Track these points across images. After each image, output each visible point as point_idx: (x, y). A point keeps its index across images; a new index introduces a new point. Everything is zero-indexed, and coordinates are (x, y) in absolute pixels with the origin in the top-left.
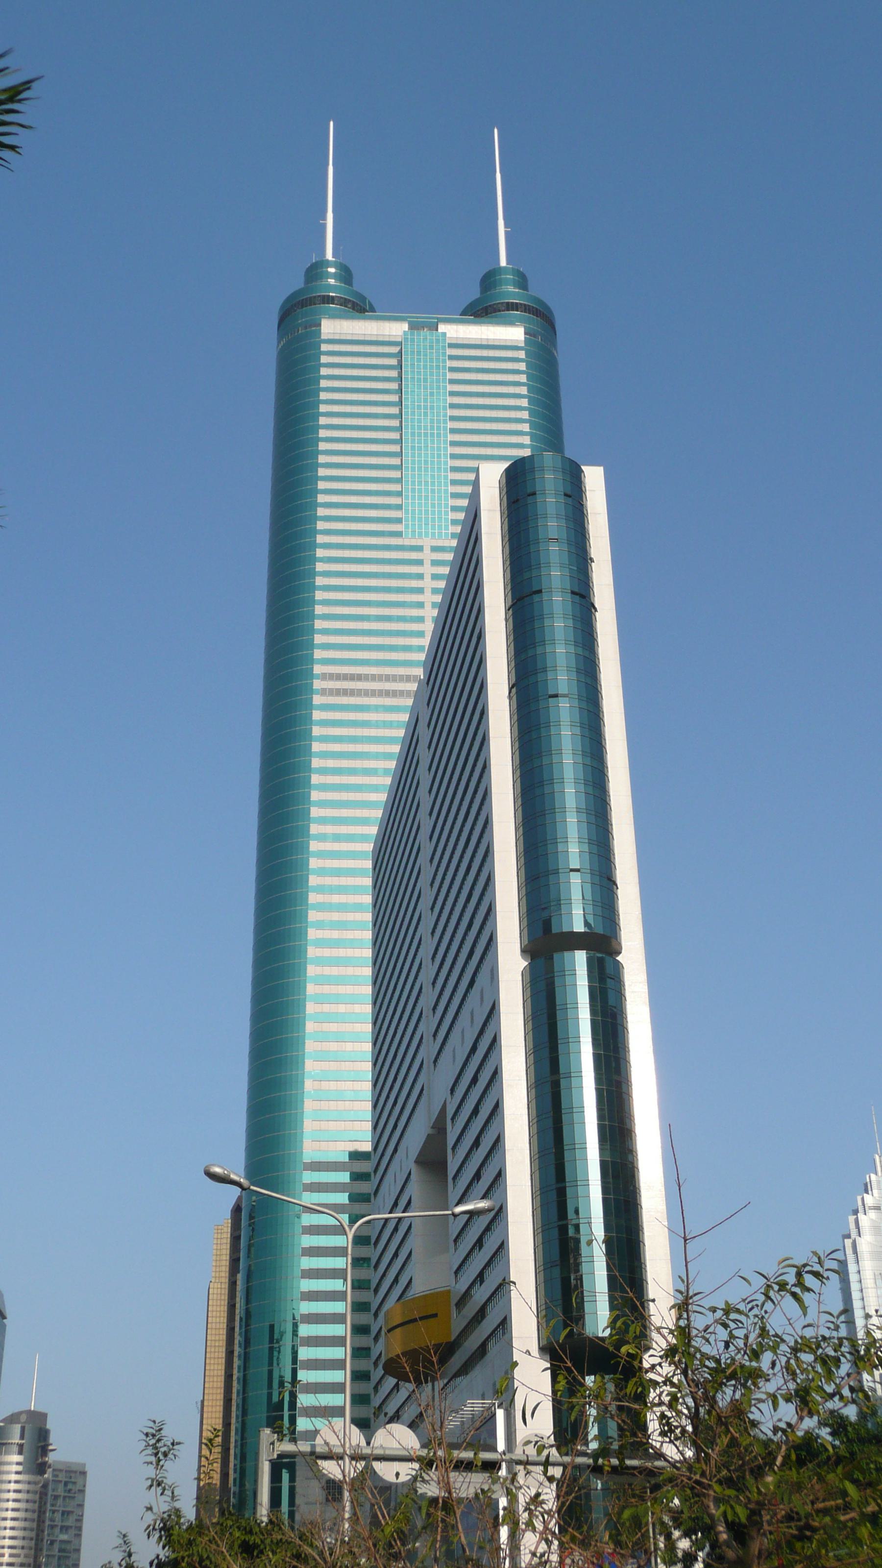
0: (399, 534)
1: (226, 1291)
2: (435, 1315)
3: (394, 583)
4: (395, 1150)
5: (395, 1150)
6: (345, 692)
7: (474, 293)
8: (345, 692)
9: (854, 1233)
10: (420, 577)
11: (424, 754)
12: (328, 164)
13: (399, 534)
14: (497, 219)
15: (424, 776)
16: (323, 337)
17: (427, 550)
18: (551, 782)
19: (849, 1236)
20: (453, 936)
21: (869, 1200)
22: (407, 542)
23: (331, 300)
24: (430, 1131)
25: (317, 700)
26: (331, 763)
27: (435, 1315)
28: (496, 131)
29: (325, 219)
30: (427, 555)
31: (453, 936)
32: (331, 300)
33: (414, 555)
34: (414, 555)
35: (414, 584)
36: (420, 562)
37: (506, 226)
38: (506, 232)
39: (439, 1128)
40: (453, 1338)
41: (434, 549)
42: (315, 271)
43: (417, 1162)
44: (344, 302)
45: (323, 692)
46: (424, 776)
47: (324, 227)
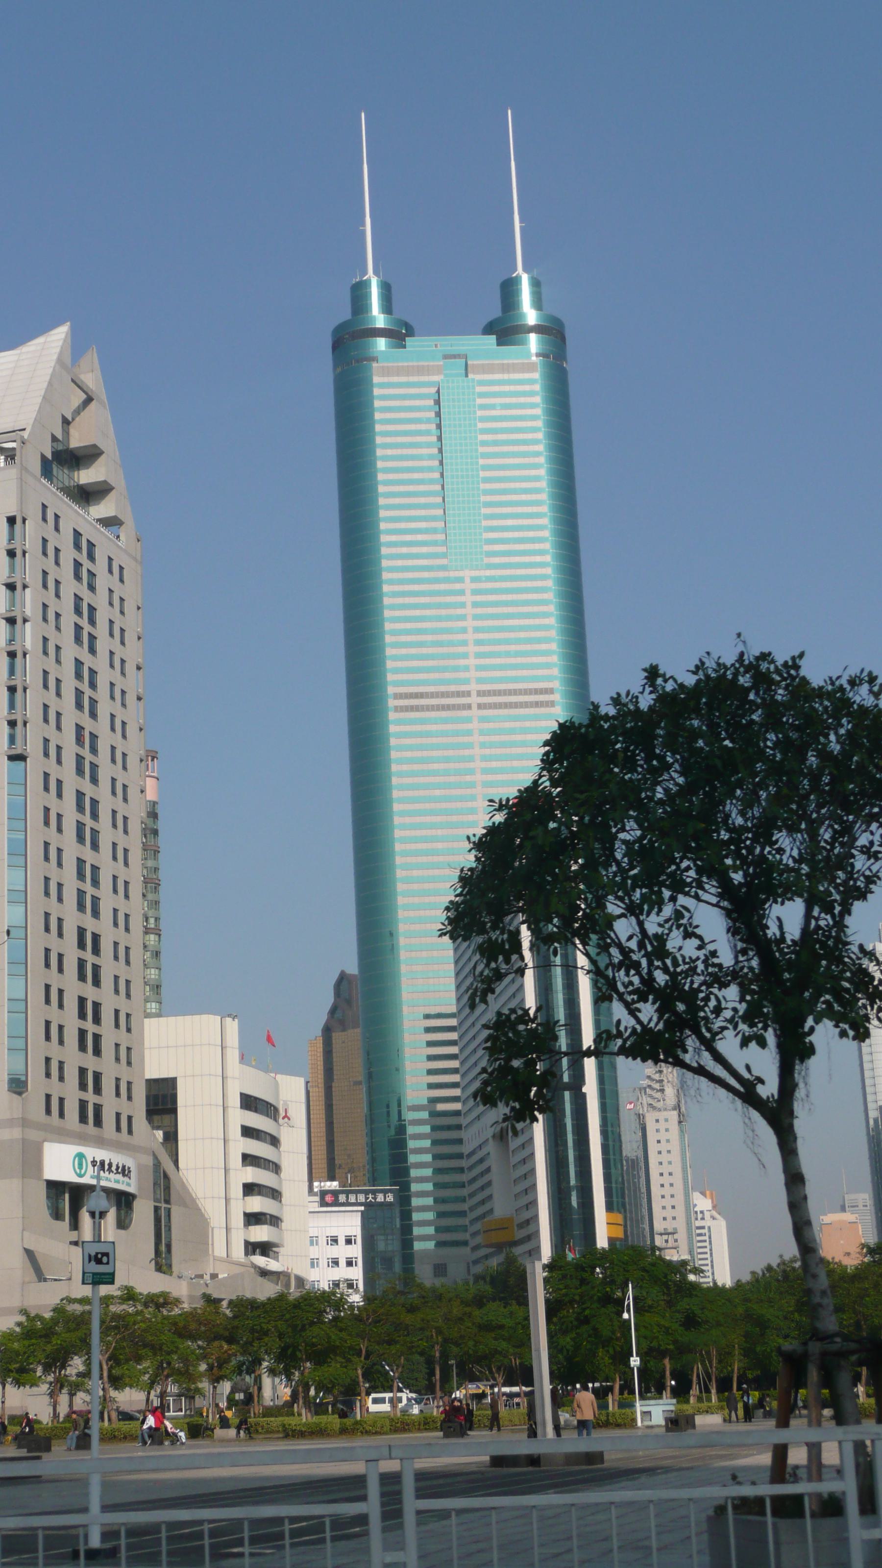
0: (444, 568)
1: (322, 1094)
3: (443, 612)
6: (412, 708)
7: (496, 312)
8: (412, 708)
10: (463, 605)
12: (362, 163)
13: (444, 568)
14: (513, 213)
16: (376, 379)
17: (467, 580)
22: (452, 574)
25: (392, 716)
26: (405, 767)
28: (509, 112)
29: (364, 225)
30: (469, 586)
33: (458, 586)
34: (458, 586)
35: (459, 611)
36: (462, 593)
37: (521, 222)
38: (521, 227)
42: (359, 293)
45: (397, 709)
47: (363, 233)
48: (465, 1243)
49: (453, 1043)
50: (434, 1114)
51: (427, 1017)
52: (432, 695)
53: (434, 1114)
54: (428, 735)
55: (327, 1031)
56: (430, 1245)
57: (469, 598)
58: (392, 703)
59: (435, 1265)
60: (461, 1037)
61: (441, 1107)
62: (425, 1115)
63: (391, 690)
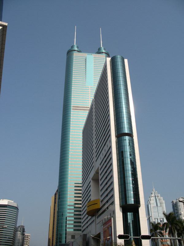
2: (97, 204)
4: (87, 178)
5: (87, 178)
7: (97, 51)
9: (150, 200)
11: (94, 110)
15: (94, 114)
18: (121, 108)
19: (149, 201)
20: (99, 141)
21: (152, 195)
23: (75, 50)
24: (95, 173)
25: (72, 110)
27: (97, 204)
31: (99, 141)
32: (75, 50)
39: (97, 173)
40: (100, 207)
41: (91, 88)
42: (73, 47)
43: (92, 179)
44: (77, 51)
46: (94, 114)
48: (80, 230)
49: (80, 200)
50: (75, 207)
51: (75, 183)
52: (81, 107)
53: (75, 207)
54: (80, 75)
55: (56, 194)
56: (72, 230)
57: (90, 91)
58: (72, 108)
59: (72, 235)
60: (82, 199)
61: (77, 206)
62: (73, 207)
63: (72, 106)
